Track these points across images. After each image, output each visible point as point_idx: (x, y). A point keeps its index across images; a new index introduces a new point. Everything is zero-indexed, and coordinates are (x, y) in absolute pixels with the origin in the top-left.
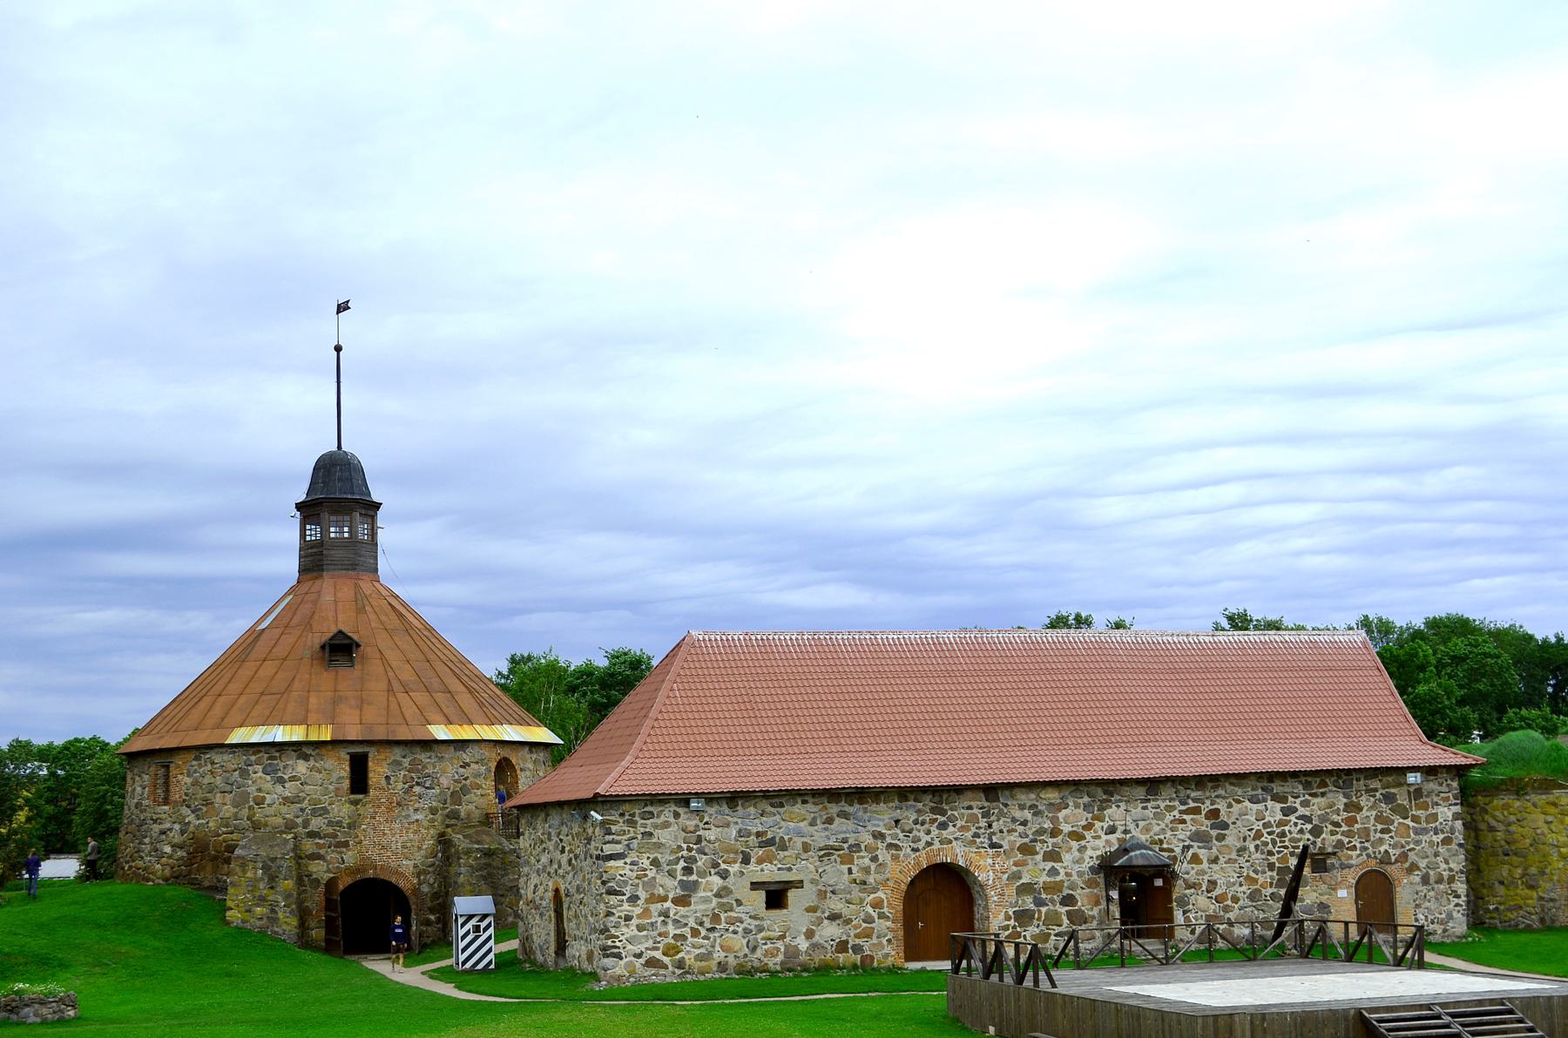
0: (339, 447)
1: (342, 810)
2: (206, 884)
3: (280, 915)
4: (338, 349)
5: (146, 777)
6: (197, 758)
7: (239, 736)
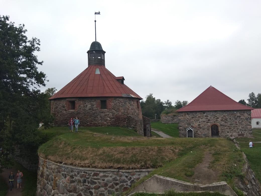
0: (96, 40)
1: (137, 111)
4: (95, 21)
6: (114, 99)
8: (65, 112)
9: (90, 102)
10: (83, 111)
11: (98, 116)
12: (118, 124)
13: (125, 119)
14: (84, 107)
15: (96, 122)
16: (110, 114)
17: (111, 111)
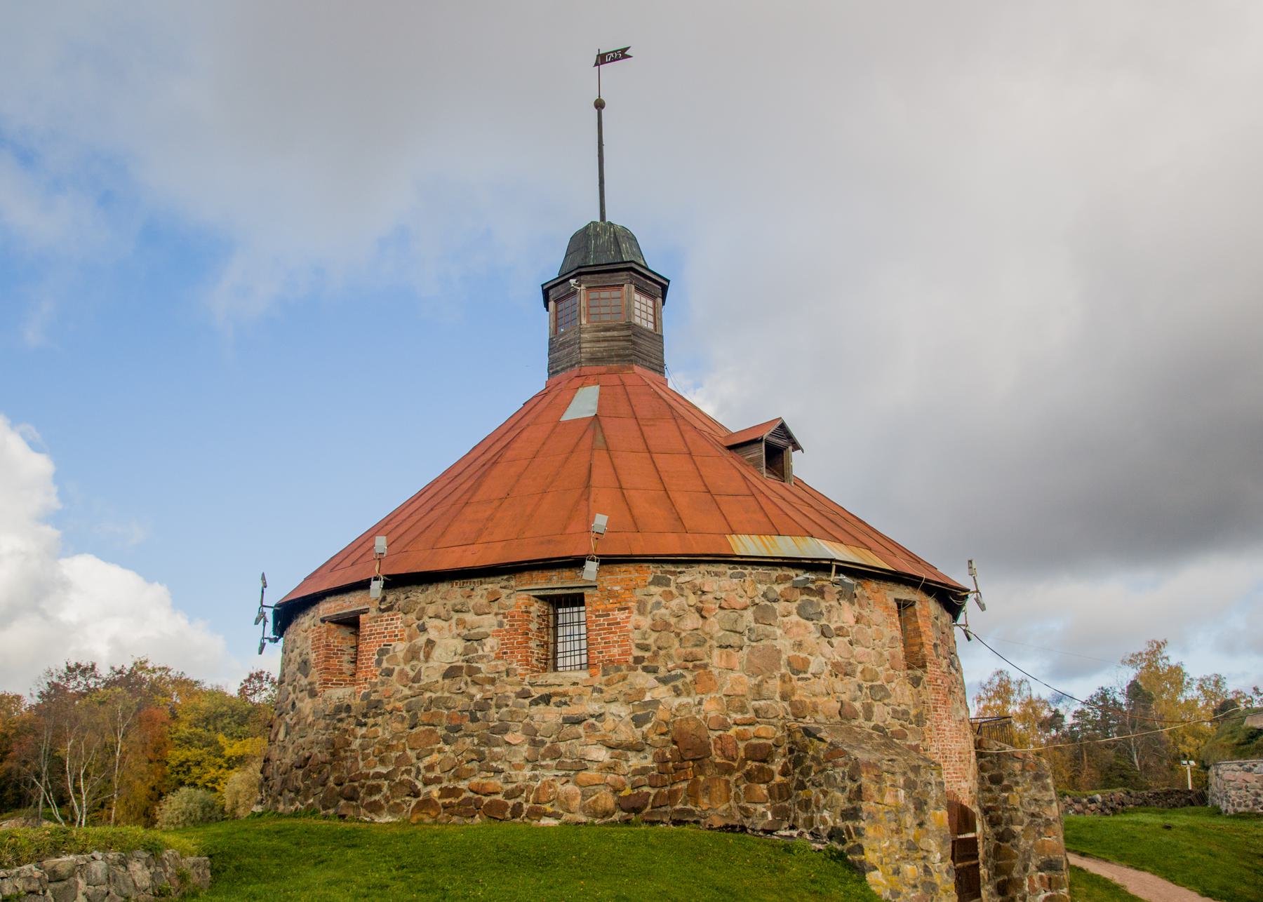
1: (902, 693)
2: (718, 822)
3: (937, 878)
5: (488, 623)
6: (657, 581)
7: (746, 545)
8: (306, 705)
9: (456, 616)
10: (407, 692)
11: (505, 730)
12: (693, 795)
13: (762, 754)
14: (412, 655)
15: (497, 782)
16: (614, 708)
17: (620, 686)
